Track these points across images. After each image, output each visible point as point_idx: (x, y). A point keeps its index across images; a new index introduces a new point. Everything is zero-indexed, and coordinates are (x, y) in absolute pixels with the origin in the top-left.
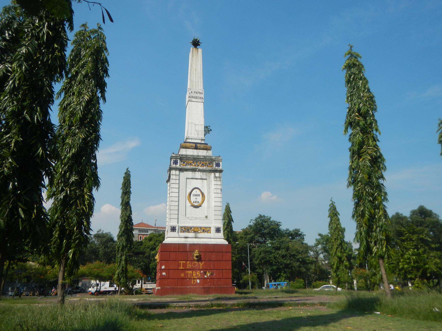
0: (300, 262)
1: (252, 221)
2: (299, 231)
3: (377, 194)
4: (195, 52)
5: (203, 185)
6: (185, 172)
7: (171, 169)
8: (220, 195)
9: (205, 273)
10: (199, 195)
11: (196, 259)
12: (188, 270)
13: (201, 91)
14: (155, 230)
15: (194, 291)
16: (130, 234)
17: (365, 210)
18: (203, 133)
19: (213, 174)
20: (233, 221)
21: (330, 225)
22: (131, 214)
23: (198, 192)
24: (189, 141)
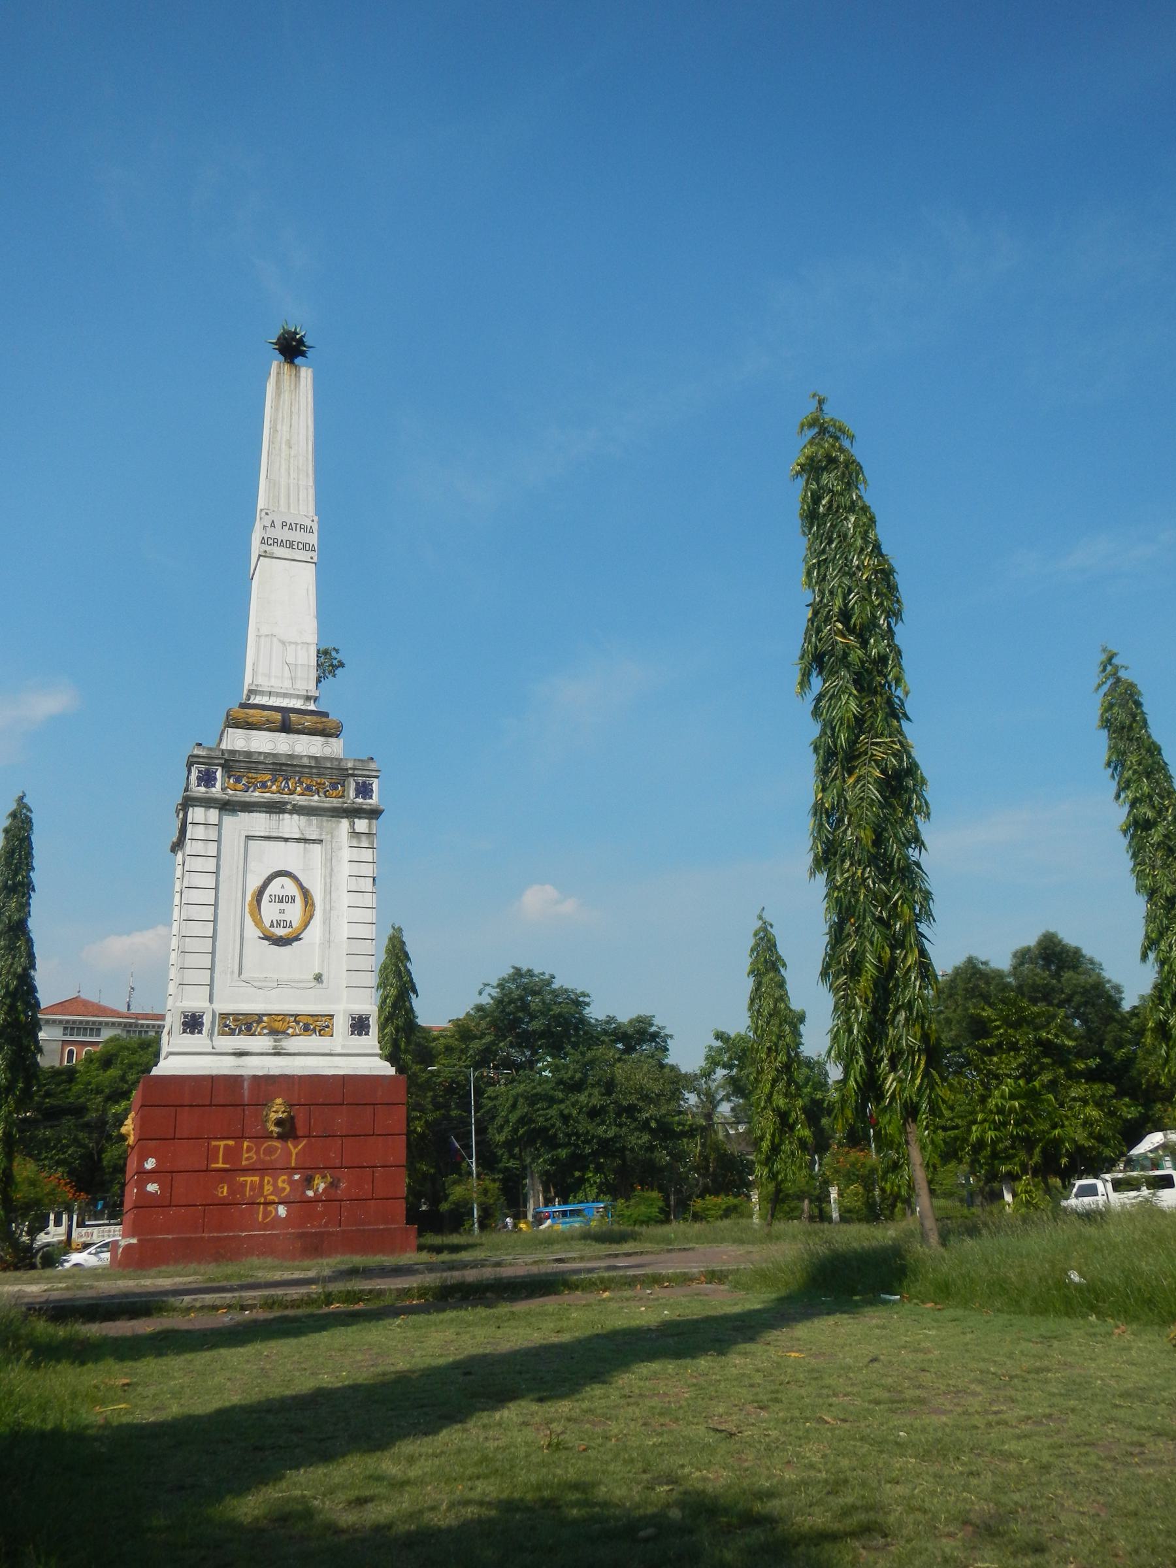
0: (652, 1131)
1: (489, 990)
2: (652, 1025)
3: (901, 897)
4: (286, 377)
5: (307, 863)
6: (243, 816)
7: (188, 802)
8: (369, 900)
9: (308, 1182)
10: (293, 899)
11: (276, 1129)
12: (246, 1171)
13: (308, 523)
14: (126, 1025)
15: (266, 1247)
16: (25, 1042)
17: (864, 952)
18: (313, 674)
19: (345, 823)
20: (415, 992)
21: (752, 1000)
22: (33, 966)
23: (291, 889)
24: (258, 700)
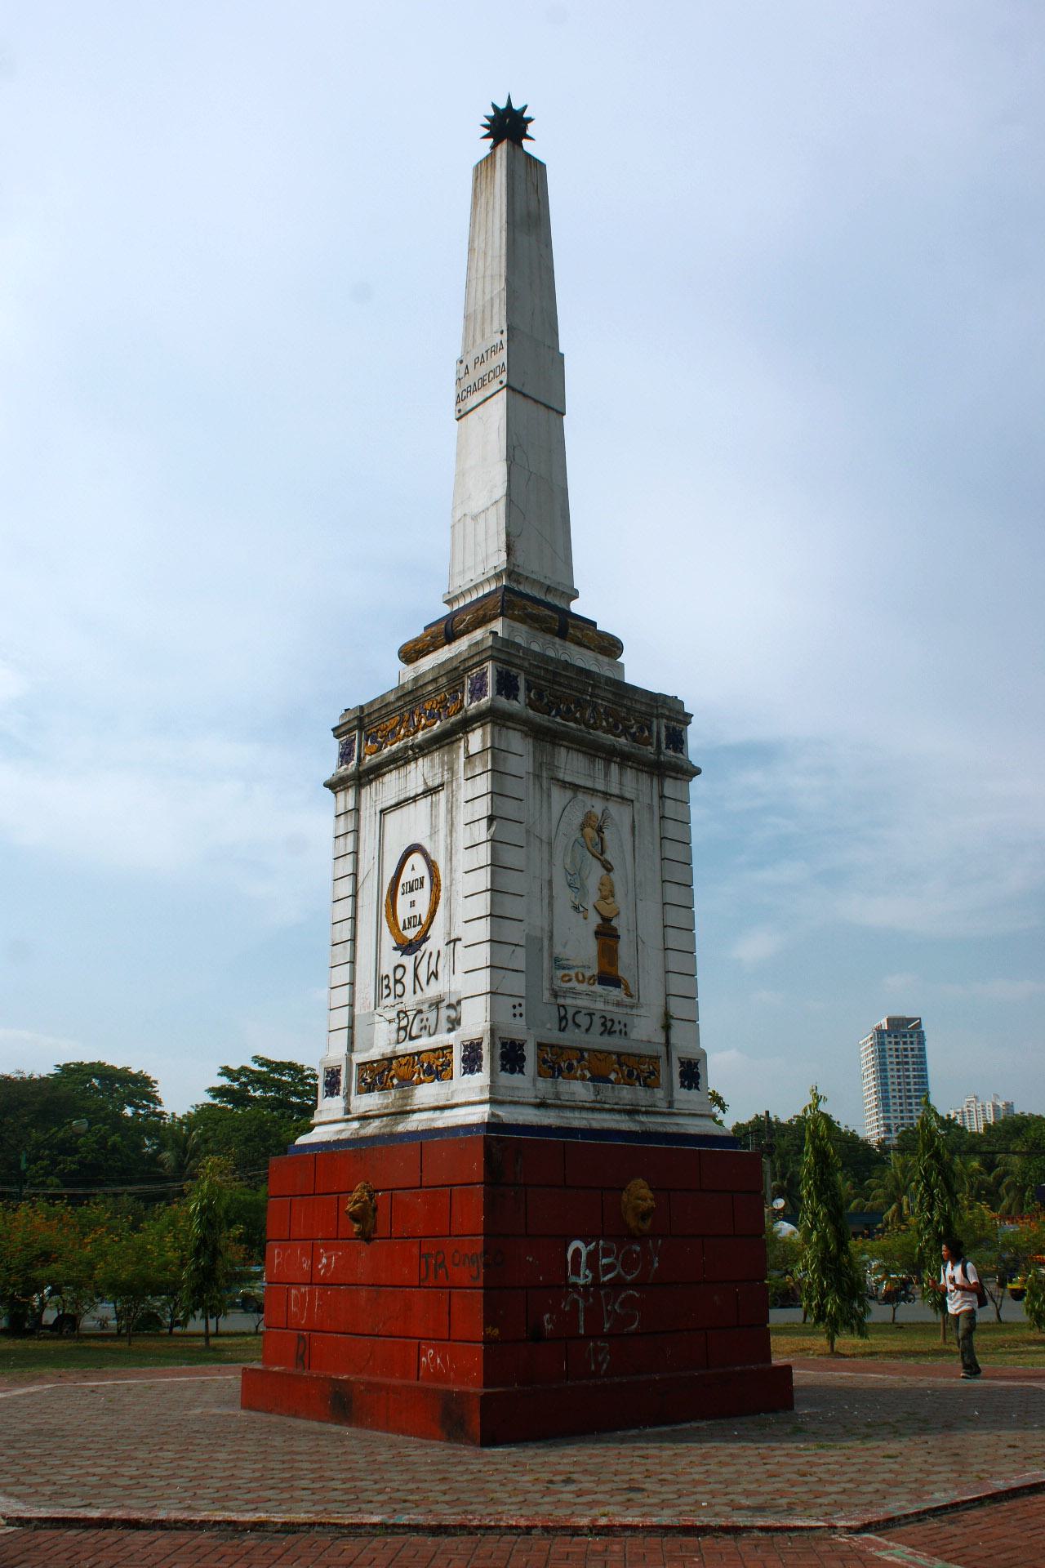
10: (422, 880)
